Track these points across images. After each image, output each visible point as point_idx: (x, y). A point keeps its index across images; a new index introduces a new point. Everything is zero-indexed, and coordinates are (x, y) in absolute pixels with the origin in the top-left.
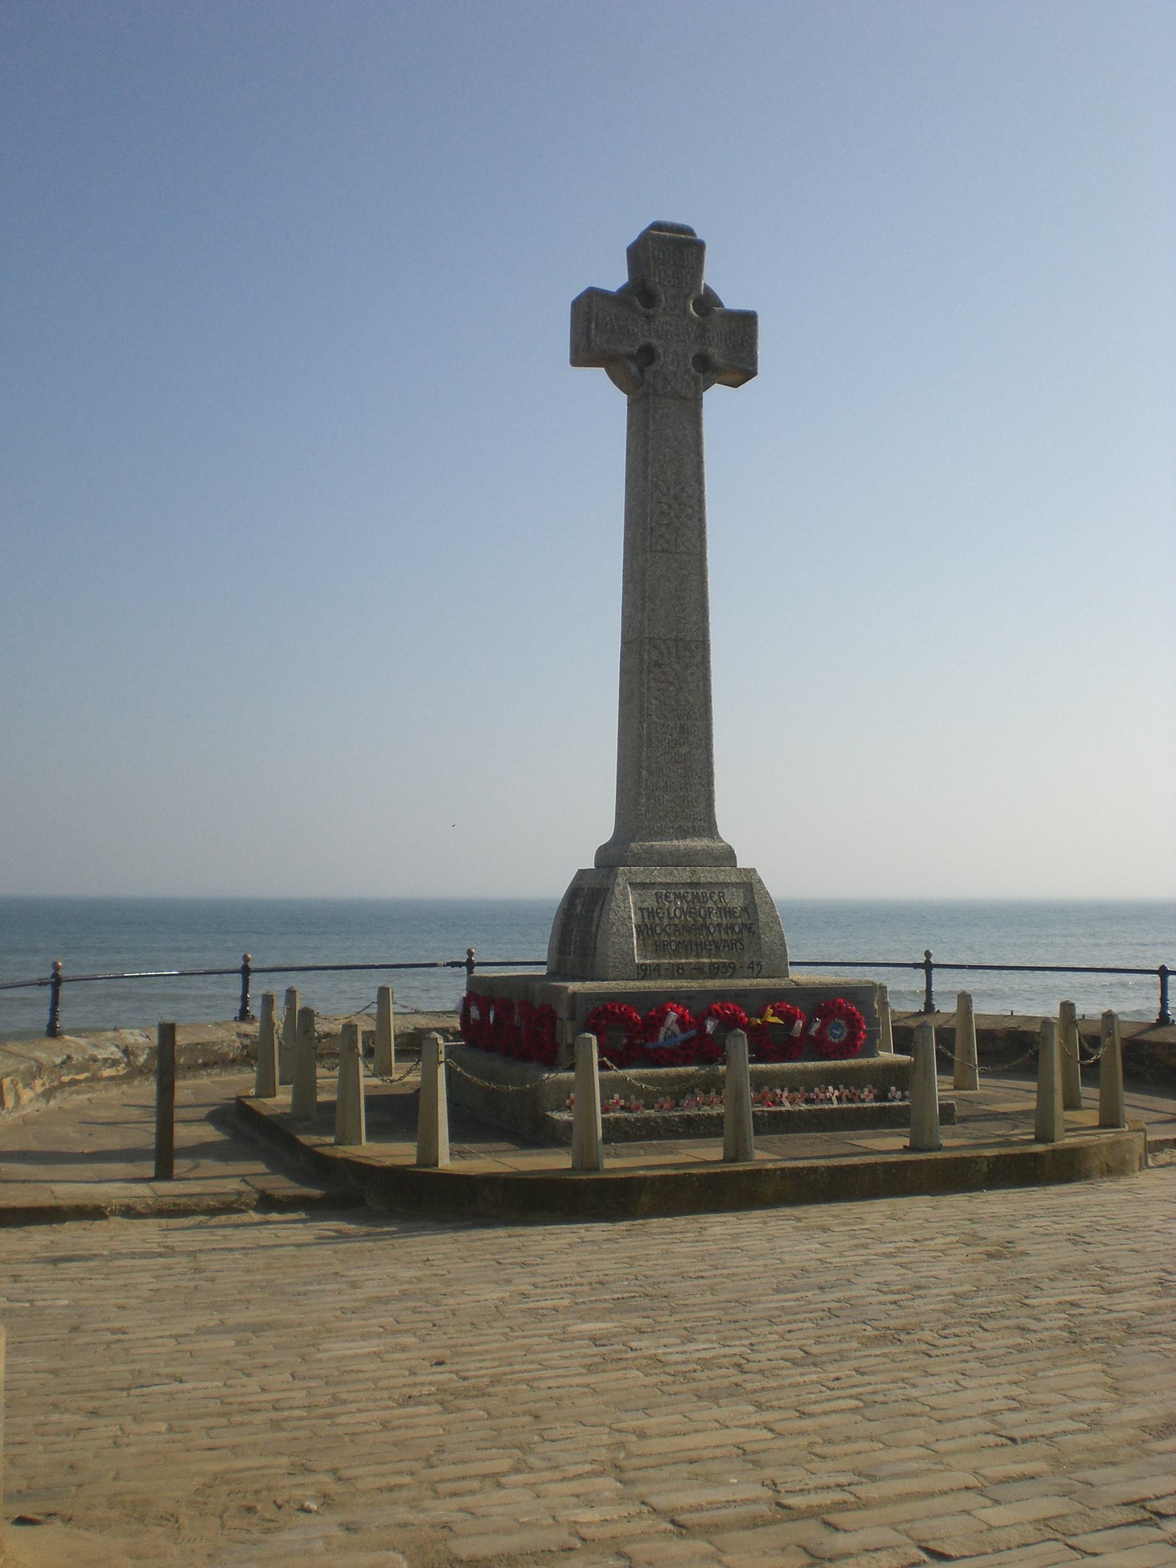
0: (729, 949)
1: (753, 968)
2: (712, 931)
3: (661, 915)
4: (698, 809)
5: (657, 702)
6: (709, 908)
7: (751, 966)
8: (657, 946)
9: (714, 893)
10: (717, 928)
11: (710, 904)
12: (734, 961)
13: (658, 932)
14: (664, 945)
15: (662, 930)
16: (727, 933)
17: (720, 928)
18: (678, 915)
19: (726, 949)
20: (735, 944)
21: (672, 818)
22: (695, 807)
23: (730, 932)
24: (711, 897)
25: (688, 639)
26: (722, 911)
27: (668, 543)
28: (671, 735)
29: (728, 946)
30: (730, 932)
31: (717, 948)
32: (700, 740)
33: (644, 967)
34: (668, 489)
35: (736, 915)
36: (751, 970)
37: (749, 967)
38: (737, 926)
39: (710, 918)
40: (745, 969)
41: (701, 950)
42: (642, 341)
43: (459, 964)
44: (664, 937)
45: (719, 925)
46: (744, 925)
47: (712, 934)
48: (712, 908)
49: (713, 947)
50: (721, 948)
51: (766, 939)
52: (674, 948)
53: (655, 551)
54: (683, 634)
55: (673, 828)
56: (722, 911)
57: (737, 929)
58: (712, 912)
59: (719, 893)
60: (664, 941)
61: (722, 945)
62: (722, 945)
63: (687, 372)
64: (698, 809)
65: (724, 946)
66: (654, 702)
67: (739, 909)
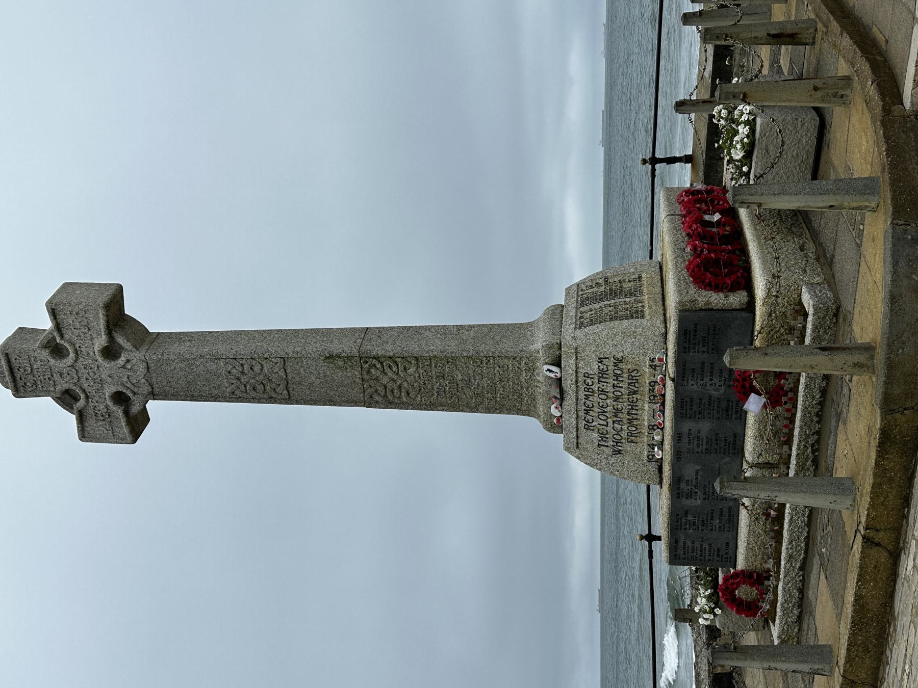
0: (637, 382)
1: (655, 366)
2: (620, 394)
3: (605, 432)
4: (510, 366)
5: (419, 396)
6: (599, 391)
7: (653, 367)
8: (632, 441)
9: (585, 381)
10: (618, 389)
11: (595, 387)
12: (647, 381)
13: (620, 438)
14: (632, 436)
15: (617, 434)
16: (622, 381)
17: (617, 387)
18: (605, 418)
19: (637, 385)
20: (633, 377)
21: (519, 388)
22: (508, 368)
23: (621, 379)
24: (588, 385)
25: (360, 369)
26: (601, 379)
27: (279, 385)
28: (446, 386)
29: (635, 383)
30: (621, 379)
31: (635, 393)
32: (448, 362)
33: (650, 457)
34: (232, 384)
35: (605, 369)
36: (657, 368)
37: (655, 370)
38: (615, 371)
39: (608, 392)
40: (656, 372)
41: (637, 406)
42: (110, 403)
43: (653, 170)
44: (624, 434)
45: (614, 386)
46: (615, 365)
47: (622, 395)
48: (599, 387)
49: (634, 396)
50: (636, 389)
51: (629, 350)
52: (634, 429)
53: (289, 395)
54: (357, 373)
55: (527, 388)
56: (601, 379)
57: (619, 372)
58: (603, 389)
59: (585, 376)
60: (628, 435)
61: (633, 388)
62: (633, 388)
63: (124, 367)
64: (510, 366)
65: (635, 386)
66: (419, 399)
67: (600, 364)
